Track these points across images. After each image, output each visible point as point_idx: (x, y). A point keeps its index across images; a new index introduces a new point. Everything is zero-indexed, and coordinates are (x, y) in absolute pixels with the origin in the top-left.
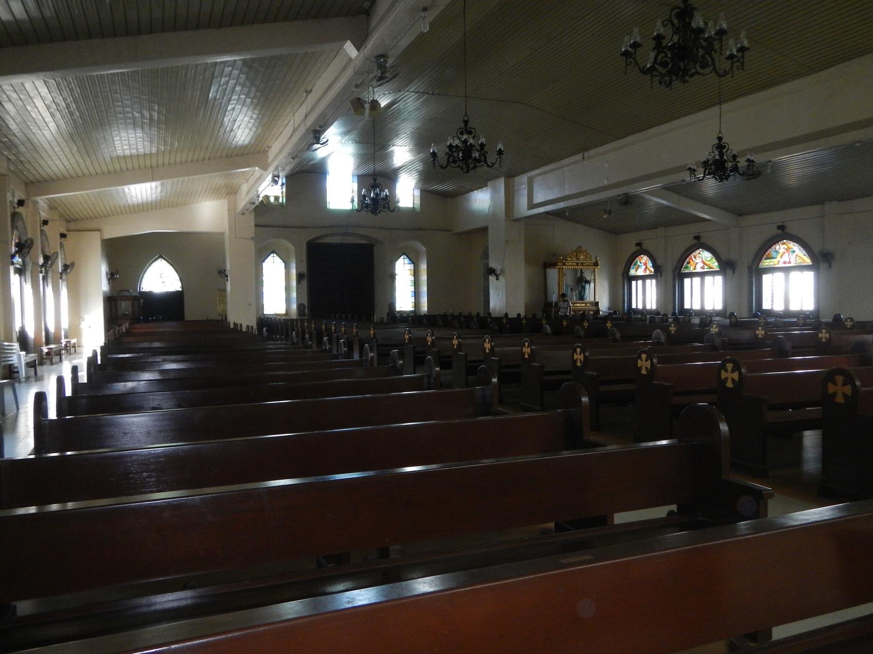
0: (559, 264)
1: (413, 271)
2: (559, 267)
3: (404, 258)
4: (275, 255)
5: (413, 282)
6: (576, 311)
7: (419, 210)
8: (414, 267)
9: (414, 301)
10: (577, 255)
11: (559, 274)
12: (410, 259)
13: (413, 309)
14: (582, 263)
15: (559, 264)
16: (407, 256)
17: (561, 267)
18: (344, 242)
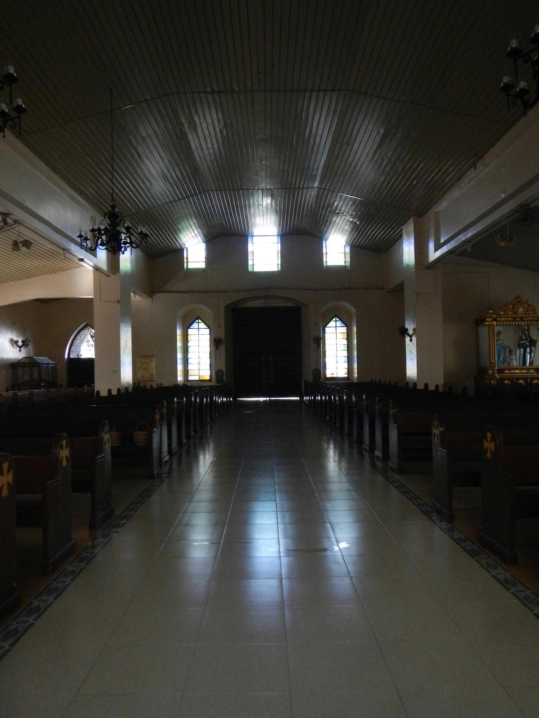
0: (488, 319)
1: (346, 335)
2: (488, 323)
3: (336, 321)
4: (200, 321)
5: (346, 346)
6: (513, 379)
7: (349, 268)
8: (348, 330)
9: (347, 367)
10: (513, 308)
11: (489, 332)
12: (343, 322)
13: (346, 376)
14: (522, 318)
15: (488, 319)
16: (339, 318)
17: (491, 323)
18: (268, 305)
